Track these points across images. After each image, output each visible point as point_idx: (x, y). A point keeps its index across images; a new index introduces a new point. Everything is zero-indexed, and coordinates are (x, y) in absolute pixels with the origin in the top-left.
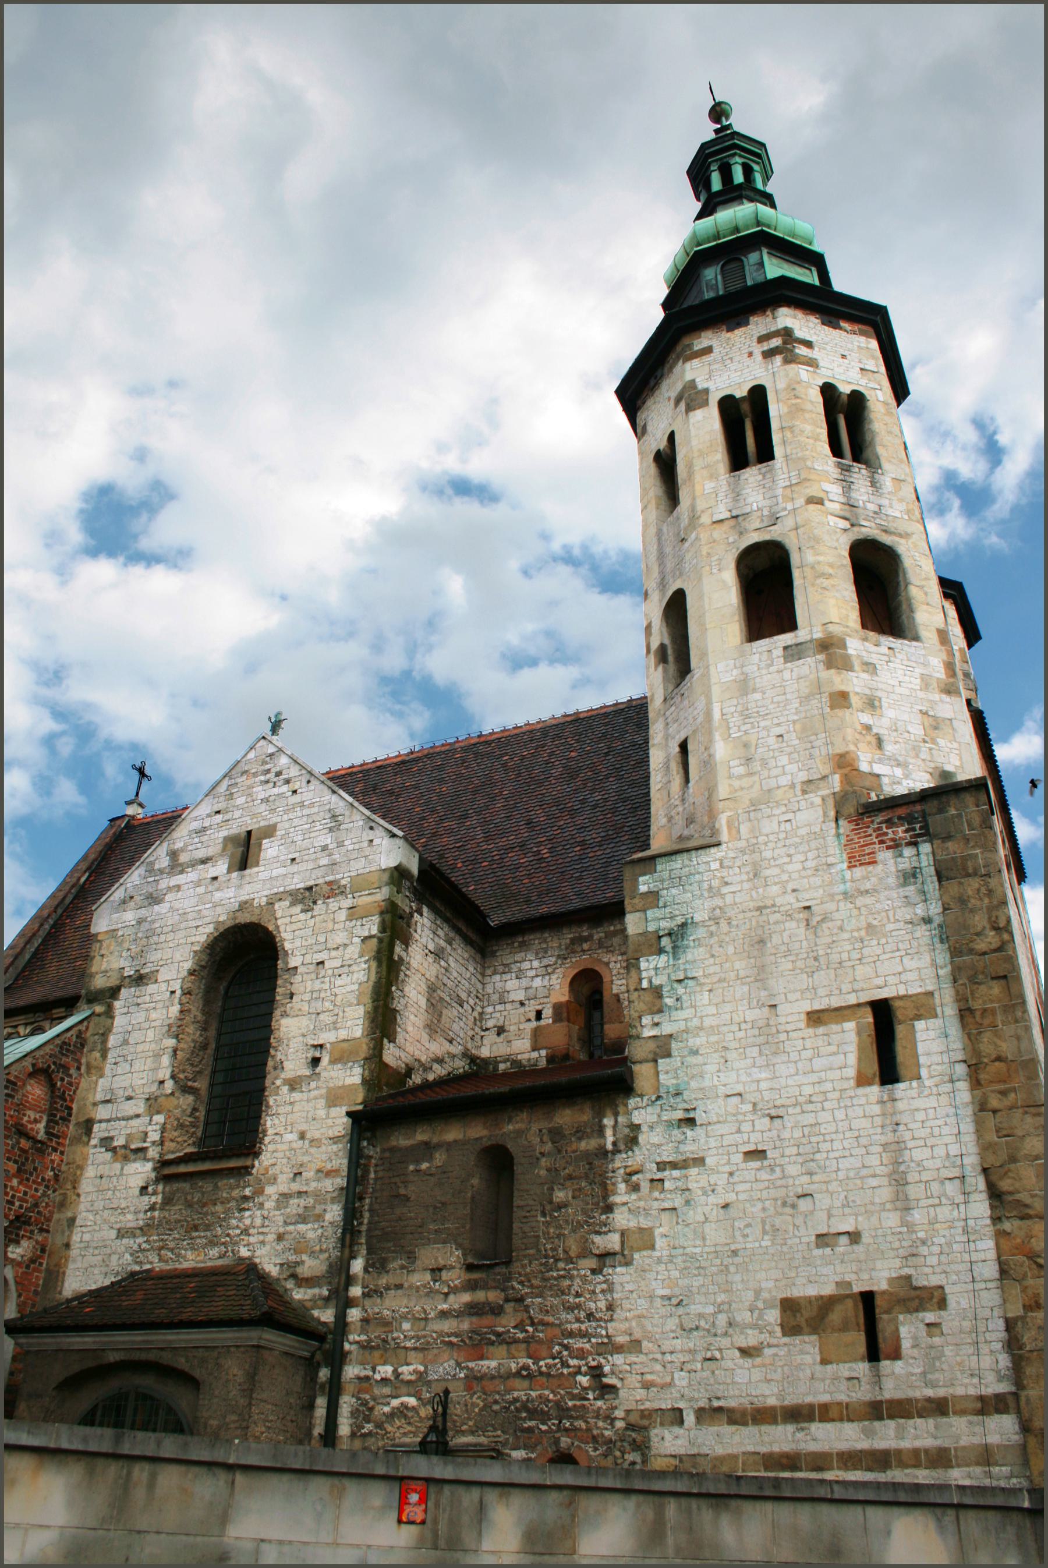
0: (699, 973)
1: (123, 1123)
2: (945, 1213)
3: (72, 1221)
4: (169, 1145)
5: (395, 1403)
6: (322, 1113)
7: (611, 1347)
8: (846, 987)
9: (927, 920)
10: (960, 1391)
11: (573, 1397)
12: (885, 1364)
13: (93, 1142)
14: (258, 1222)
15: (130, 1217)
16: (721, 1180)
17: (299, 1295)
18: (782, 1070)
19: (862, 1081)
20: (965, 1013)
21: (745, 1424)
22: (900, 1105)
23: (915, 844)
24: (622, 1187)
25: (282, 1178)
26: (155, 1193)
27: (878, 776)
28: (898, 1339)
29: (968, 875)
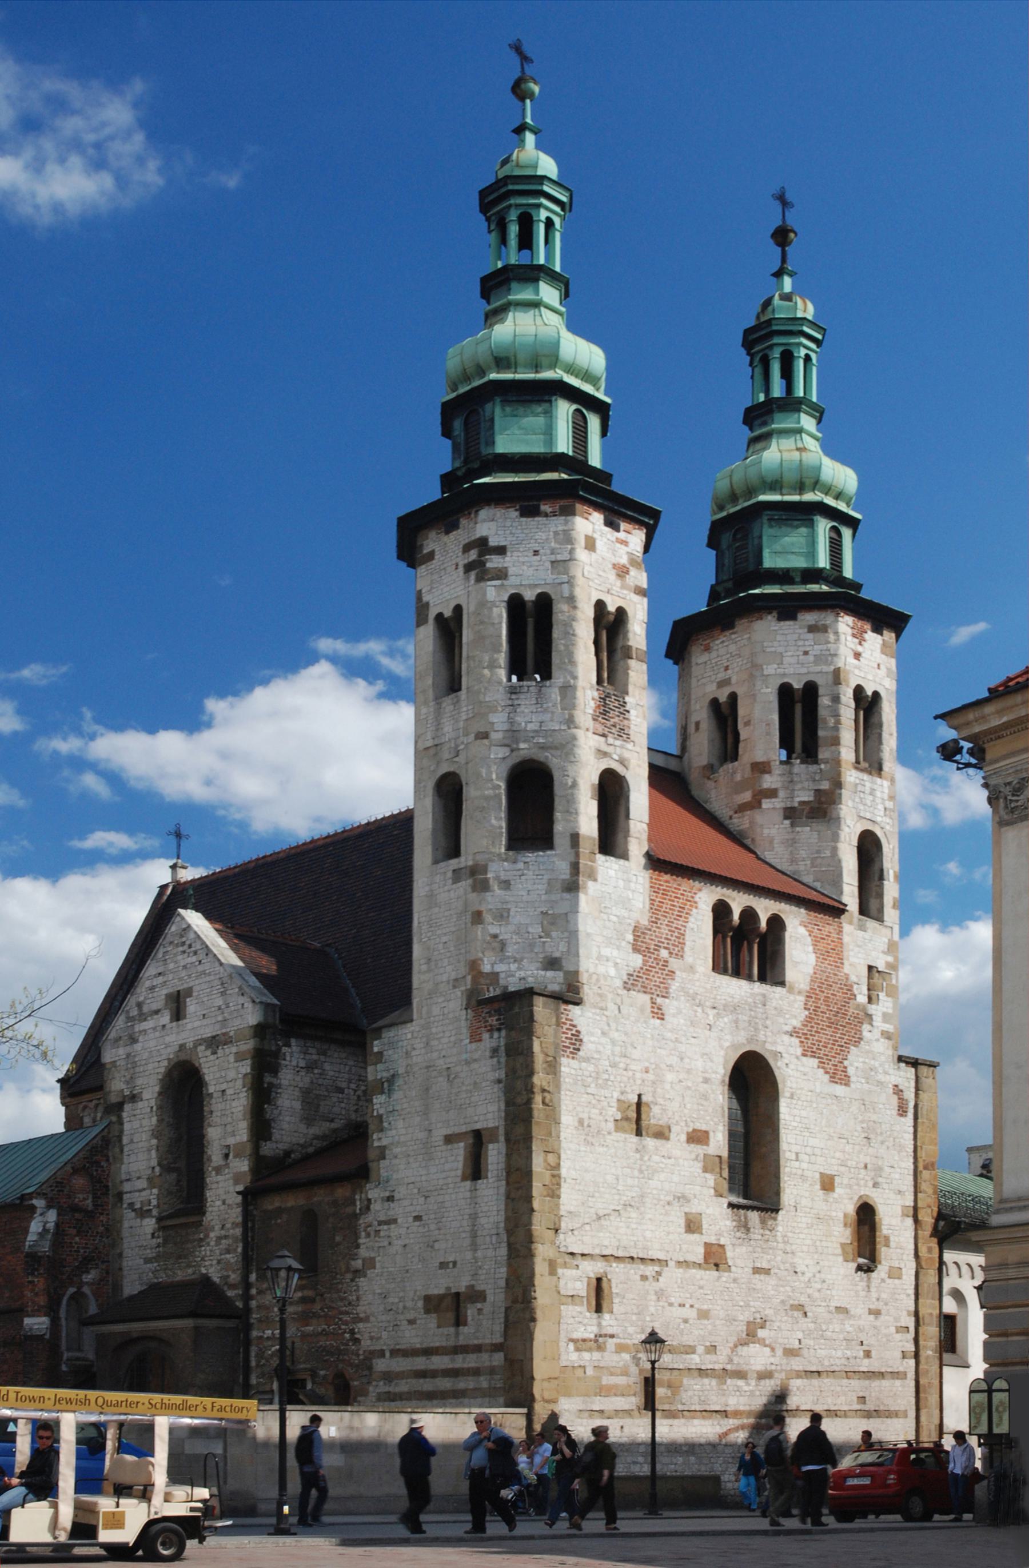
0: (398, 1108)
1: (137, 1194)
2: (490, 1253)
3: (120, 1255)
4: (166, 1206)
5: (273, 1349)
6: (231, 1189)
7: (358, 1320)
8: (462, 1121)
9: (499, 1081)
10: (488, 1341)
11: (343, 1344)
12: (461, 1328)
13: (125, 1206)
14: (208, 1253)
15: (148, 1251)
16: (403, 1231)
17: (230, 1293)
18: (433, 1170)
19: (464, 1178)
20: (508, 1140)
21: (407, 1357)
22: (479, 1193)
23: (499, 1030)
24: (363, 1234)
25: (217, 1228)
26: (158, 1237)
27: (498, 973)
28: (466, 1316)
29: (520, 1054)
